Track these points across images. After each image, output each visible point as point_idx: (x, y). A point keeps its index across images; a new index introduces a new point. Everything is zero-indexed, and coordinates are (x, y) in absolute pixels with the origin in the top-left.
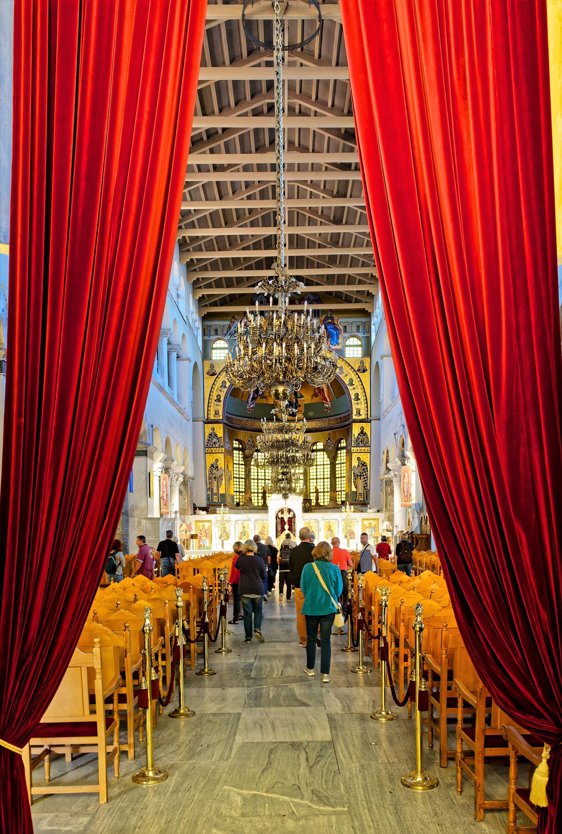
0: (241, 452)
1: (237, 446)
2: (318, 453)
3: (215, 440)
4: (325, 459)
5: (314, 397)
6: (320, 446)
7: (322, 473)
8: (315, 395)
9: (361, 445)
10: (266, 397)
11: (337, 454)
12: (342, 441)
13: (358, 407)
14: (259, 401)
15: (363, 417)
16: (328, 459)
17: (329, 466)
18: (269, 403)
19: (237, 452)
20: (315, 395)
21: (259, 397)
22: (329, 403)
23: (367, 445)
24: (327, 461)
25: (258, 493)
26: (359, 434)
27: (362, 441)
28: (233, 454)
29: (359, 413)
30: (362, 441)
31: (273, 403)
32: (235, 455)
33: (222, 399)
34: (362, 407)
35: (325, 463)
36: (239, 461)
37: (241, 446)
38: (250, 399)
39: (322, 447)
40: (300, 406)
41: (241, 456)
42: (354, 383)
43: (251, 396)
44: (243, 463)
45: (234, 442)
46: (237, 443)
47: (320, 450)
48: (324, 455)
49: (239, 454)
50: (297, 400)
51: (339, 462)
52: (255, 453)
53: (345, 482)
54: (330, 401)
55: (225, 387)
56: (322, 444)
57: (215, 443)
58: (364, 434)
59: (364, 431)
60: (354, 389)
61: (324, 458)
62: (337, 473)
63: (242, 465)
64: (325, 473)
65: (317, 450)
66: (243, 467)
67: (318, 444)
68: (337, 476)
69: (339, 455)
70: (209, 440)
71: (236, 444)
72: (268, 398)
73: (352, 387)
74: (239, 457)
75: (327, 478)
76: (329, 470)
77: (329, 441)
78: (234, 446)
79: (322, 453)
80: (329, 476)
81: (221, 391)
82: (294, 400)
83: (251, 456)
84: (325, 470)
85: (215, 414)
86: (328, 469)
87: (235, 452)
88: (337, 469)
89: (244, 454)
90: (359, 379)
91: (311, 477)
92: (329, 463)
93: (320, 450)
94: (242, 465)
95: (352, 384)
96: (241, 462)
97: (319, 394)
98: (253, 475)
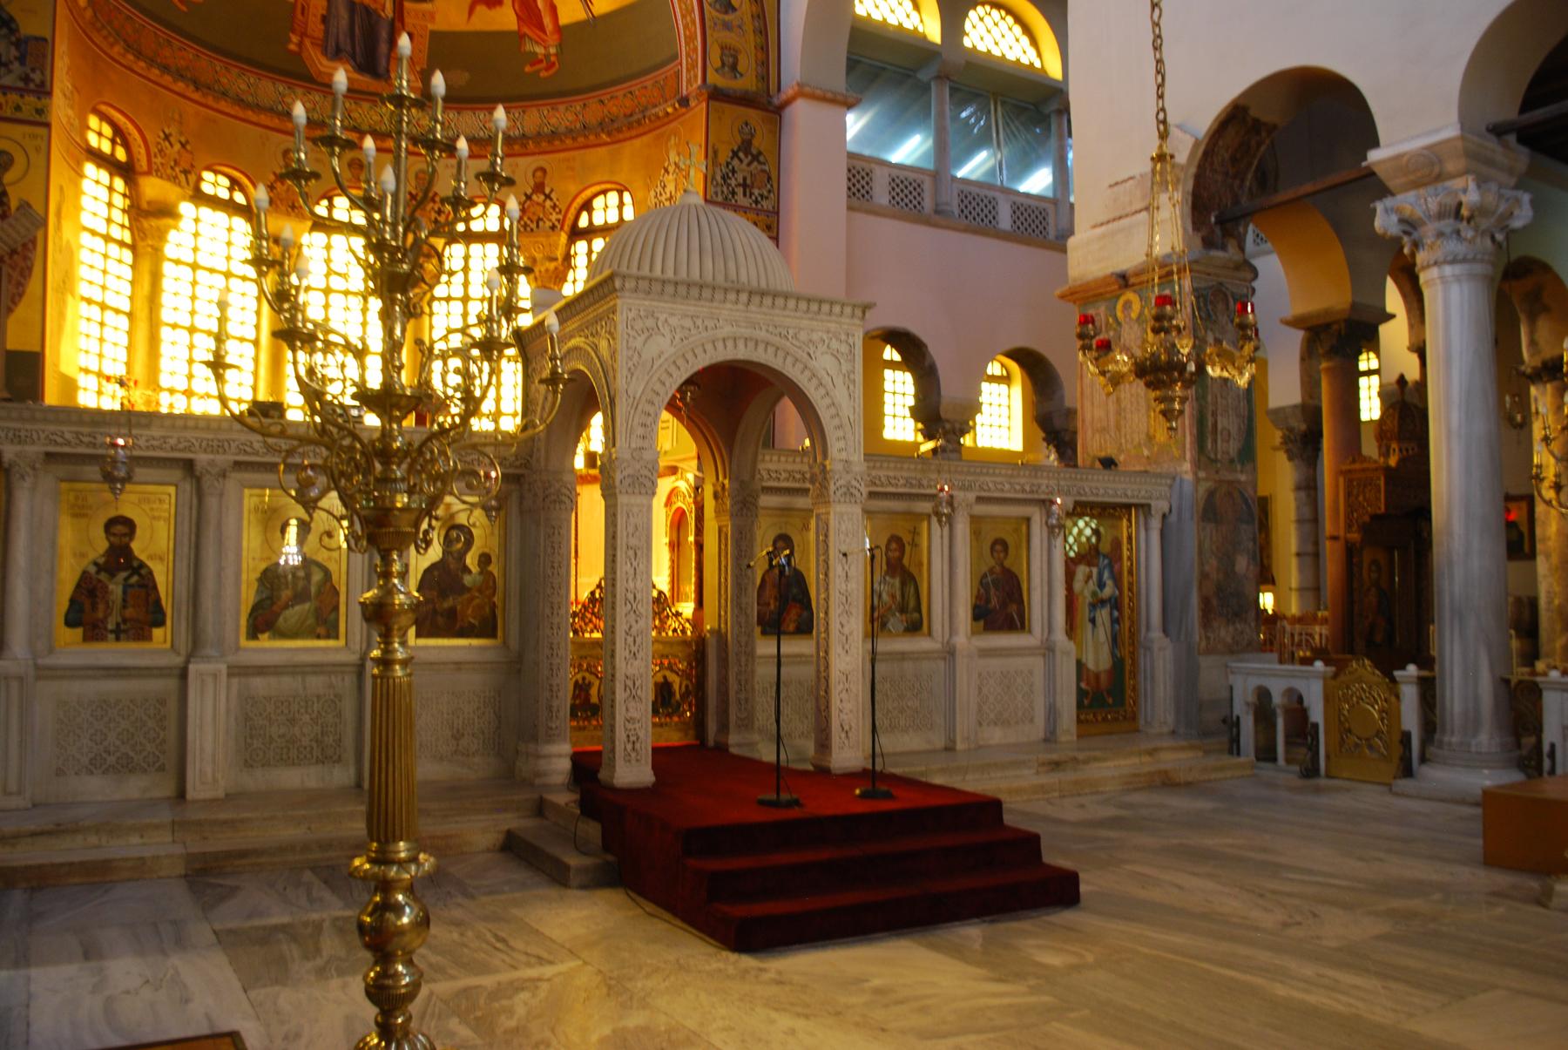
0: (119, 184)
1: (106, 147)
2: (476, 248)
5: (481, 9)
9: (741, 199)
11: (568, 257)
12: (598, 203)
13: (731, 38)
15: (747, 82)
19: (104, 175)
22: (552, 39)
23: (764, 203)
25: (188, 393)
26: (735, 154)
27: (744, 185)
28: (81, 175)
29: (734, 67)
30: (744, 185)
32: (86, 185)
34: (747, 44)
36: (109, 220)
37: (121, 154)
41: (119, 201)
44: (127, 236)
45: (93, 121)
46: (107, 130)
47: (484, 237)
49: (111, 189)
52: (186, 208)
58: (756, 158)
59: (756, 142)
63: (122, 244)
65: (470, 237)
66: (127, 255)
71: (99, 136)
74: (110, 205)
78: (93, 140)
83: (167, 212)
87: (90, 168)
89: (133, 194)
93: (484, 237)
94: (122, 244)
96: (117, 233)
98: (173, 305)
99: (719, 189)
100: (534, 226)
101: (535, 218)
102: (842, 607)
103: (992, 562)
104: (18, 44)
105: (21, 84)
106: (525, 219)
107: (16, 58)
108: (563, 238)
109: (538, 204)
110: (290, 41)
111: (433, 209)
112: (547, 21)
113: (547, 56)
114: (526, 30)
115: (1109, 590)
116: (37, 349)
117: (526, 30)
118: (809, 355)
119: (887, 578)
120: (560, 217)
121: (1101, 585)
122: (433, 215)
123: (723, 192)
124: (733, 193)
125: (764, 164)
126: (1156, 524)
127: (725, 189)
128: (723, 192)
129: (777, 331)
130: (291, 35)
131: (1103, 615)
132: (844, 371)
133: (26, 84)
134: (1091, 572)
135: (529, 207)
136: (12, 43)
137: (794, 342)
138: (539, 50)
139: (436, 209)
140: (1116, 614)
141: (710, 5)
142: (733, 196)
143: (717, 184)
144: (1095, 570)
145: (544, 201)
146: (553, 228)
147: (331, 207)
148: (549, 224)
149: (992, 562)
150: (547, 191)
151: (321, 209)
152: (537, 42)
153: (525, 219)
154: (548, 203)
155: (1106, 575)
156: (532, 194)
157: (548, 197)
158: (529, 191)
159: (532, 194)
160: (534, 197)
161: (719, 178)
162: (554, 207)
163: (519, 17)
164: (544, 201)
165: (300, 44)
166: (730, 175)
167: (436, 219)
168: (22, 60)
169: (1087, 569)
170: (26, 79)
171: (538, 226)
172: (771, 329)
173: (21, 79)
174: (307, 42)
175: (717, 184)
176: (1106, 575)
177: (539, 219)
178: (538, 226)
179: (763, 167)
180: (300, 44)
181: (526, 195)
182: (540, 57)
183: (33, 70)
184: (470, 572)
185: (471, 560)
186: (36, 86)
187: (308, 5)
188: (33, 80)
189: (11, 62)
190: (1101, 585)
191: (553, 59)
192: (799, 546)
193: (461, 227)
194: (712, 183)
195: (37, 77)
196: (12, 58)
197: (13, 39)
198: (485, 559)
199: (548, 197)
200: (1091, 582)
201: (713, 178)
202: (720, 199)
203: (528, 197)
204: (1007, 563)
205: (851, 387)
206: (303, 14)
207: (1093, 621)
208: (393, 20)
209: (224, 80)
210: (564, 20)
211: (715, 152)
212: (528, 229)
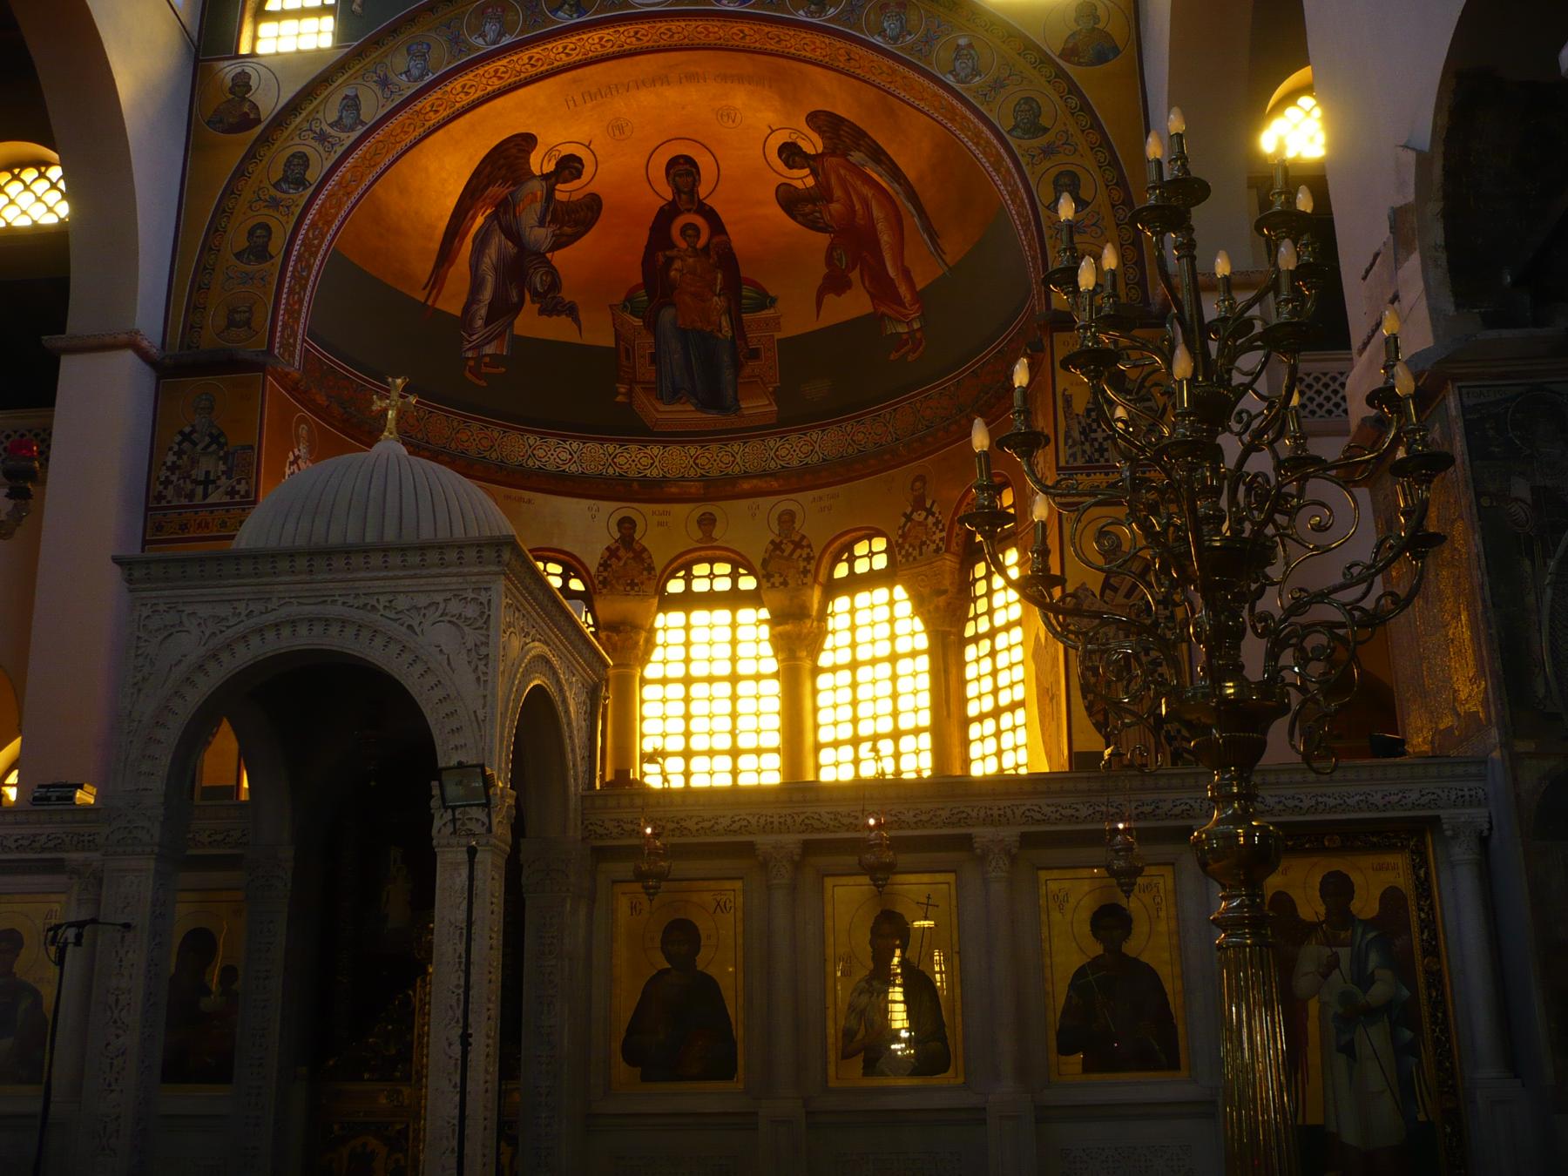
2: (863, 598)
3: (208, 465)
4: (902, 627)
5: (830, 299)
6: (872, 555)
7: (886, 706)
8: (835, 283)
10: (571, 311)
14: (530, 323)
16: (918, 624)
17: (924, 662)
18: (588, 339)
20: (835, 283)
21: (530, 308)
24: (914, 633)
31: (609, 342)
33: (277, 245)
35: (903, 646)
38: (483, 312)
39: (881, 562)
40: (755, 354)
42: (1044, 121)
43: (487, 295)
47: (872, 580)
48: (891, 603)
50: (738, 325)
51: (984, 625)
53: (1022, 736)
54: (918, 297)
55: (301, 183)
56: (880, 544)
57: (207, 482)
60: (1048, 151)
61: (892, 621)
62: (971, 690)
64: (905, 703)
65: (855, 583)
67: (861, 548)
68: (973, 710)
69: (981, 588)
70: (173, 468)
72: (582, 316)
73: (1036, 143)
75: (917, 731)
76: (925, 681)
77: (919, 516)
79: (881, 594)
80: (925, 719)
81: (275, 204)
82: (725, 322)
84: (904, 685)
85: (231, 323)
86: (917, 677)
88: (971, 672)
90: (1074, 101)
91: (825, 735)
92: (923, 642)
95: (1036, 129)
97: (855, 276)
99: (1078, 449)
100: (916, 553)
101: (917, 543)
102: (450, 1013)
103: (1098, 949)
104: (225, 459)
105: (227, 499)
106: (907, 546)
107: (223, 472)
108: (949, 562)
109: (920, 524)
110: (619, 394)
111: (801, 556)
112: (903, 290)
113: (912, 332)
114: (883, 309)
115: (1380, 991)
116: (234, 783)
117: (883, 309)
118: (410, 627)
119: (875, 983)
120: (944, 534)
121: (1364, 980)
122: (802, 564)
123: (1084, 452)
124: (1102, 450)
125: (1149, 400)
126: (1463, 852)
127: (1087, 447)
128: (1084, 452)
129: (361, 602)
130: (618, 385)
131: (1374, 1039)
132: (470, 645)
133: (232, 498)
134: (1336, 955)
135: (909, 530)
136: (220, 458)
137: (387, 613)
138: (902, 329)
139: (804, 556)
140: (1407, 1034)
141: (1048, 207)
142: (1102, 456)
143: (1074, 441)
144: (1344, 953)
145: (926, 518)
146: (938, 550)
147: (689, 579)
148: (933, 547)
149: (1098, 949)
150: (928, 505)
151: (675, 586)
152: (900, 321)
153: (907, 546)
154: (931, 520)
155: (1373, 959)
156: (912, 513)
157: (930, 512)
158: (908, 512)
159: (912, 513)
160: (915, 516)
161: (1076, 434)
162: (936, 524)
163: (873, 297)
164: (926, 518)
165: (630, 393)
166: (1094, 426)
167: (805, 567)
168: (228, 473)
169: (1327, 951)
170: (232, 492)
171: (921, 554)
172: (351, 601)
173: (227, 493)
174: (638, 388)
175: (1074, 441)
176: (1373, 959)
177: (924, 543)
178: (921, 554)
179: (1147, 404)
180: (630, 393)
181: (905, 515)
182: (905, 337)
183: (239, 482)
184: (208, 992)
185: (214, 979)
186: (242, 497)
187: (634, 350)
188: (238, 492)
189: (219, 478)
190: (1364, 980)
191: (918, 335)
192: (709, 937)
193: (841, 571)
194: (1066, 444)
195: (242, 488)
196: (220, 474)
197: (222, 453)
198: (229, 973)
199: (930, 512)
200: (1336, 975)
201: (1067, 437)
202: (1080, 462)
203: (909, 518)
204: (1131, 947)
205: (481, 667)
206: (628, 357)
207: (1349, 1050)
208: (732, 337)
209: (541, 453)
210: (919, 288)
211: (1068, 401)
212: (911, 559)
